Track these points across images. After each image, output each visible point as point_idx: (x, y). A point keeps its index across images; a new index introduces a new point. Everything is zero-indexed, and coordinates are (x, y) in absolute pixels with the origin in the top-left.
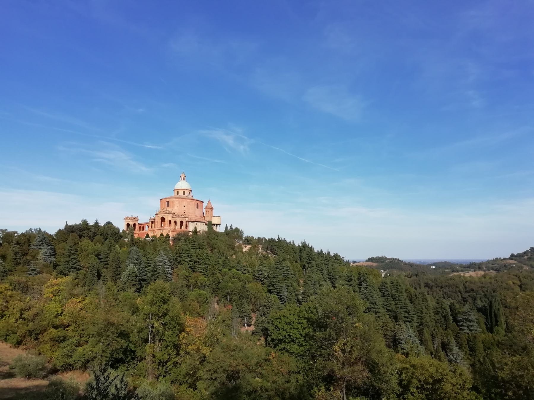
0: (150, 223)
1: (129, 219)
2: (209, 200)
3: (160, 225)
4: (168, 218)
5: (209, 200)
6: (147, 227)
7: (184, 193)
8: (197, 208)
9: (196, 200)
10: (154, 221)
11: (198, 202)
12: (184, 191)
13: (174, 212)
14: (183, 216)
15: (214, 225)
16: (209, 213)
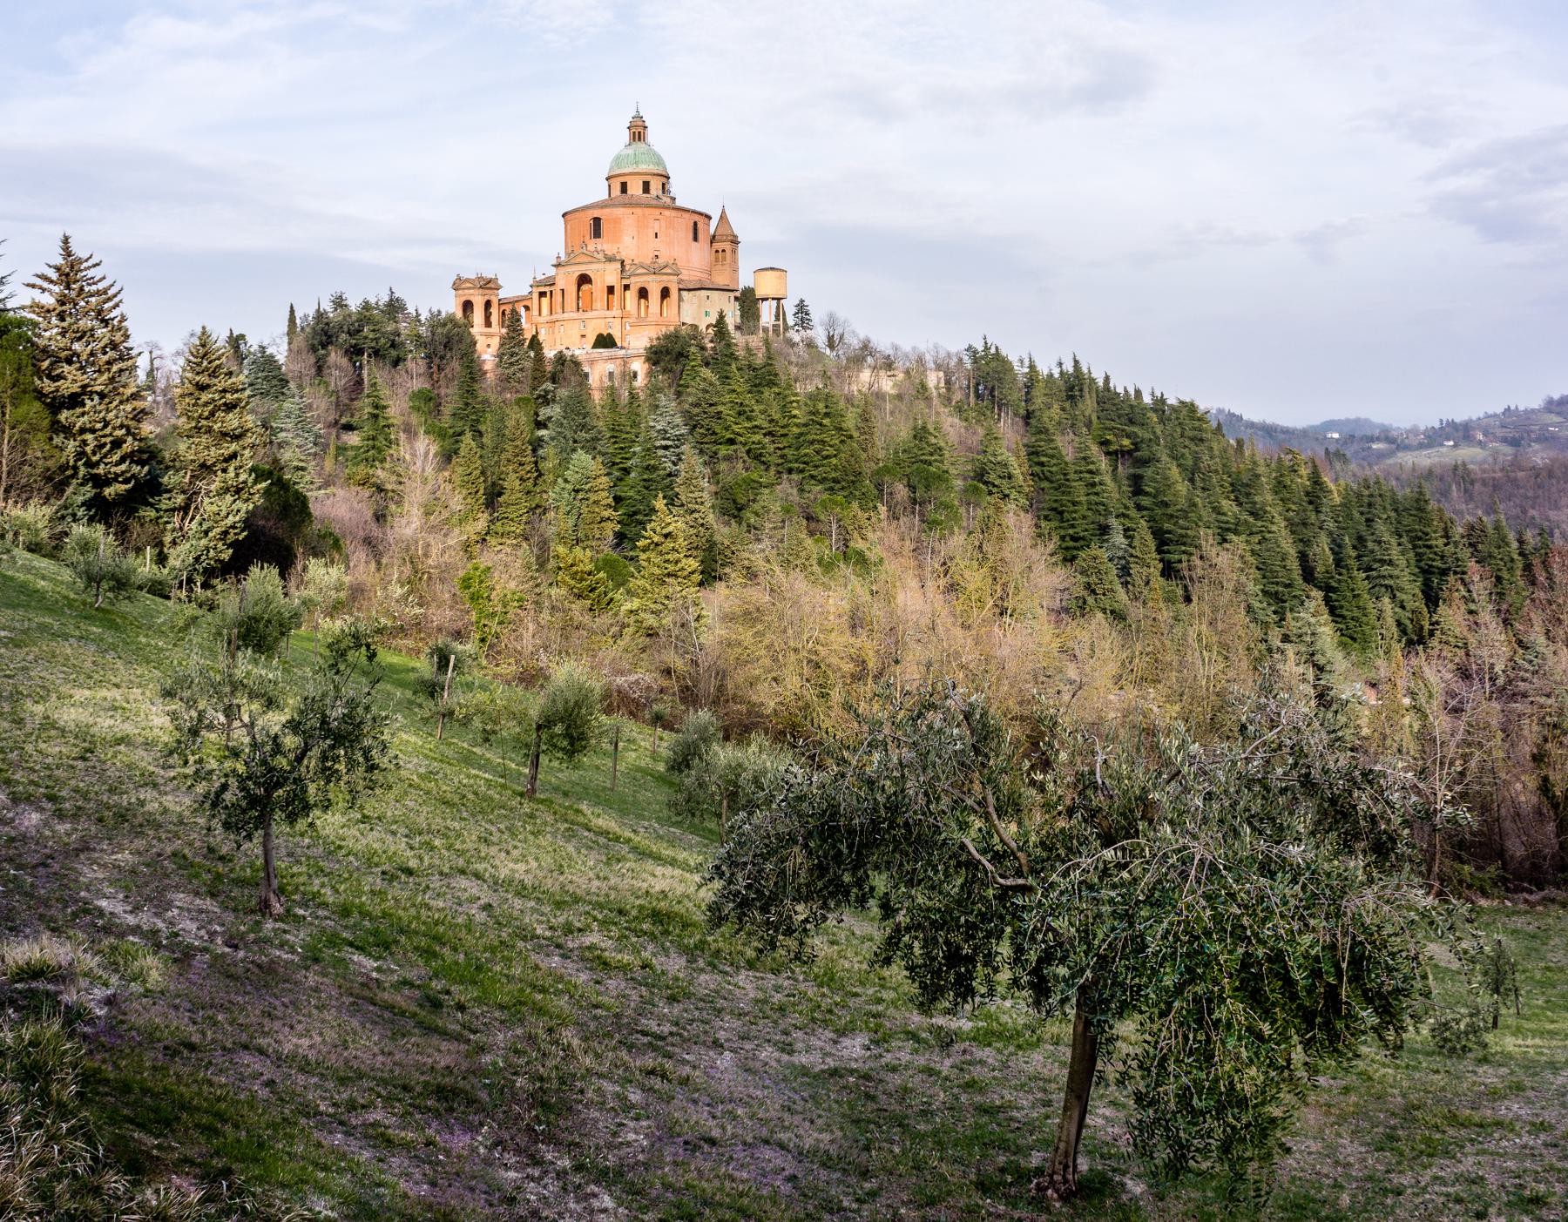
0: (536, 296)
1: (468, 285)
2: (723, 212)
3: (575, 305)
4: (608, 275)
5: (723, 212)
6: (522, 311)
7: (646, 187)
8: (696, 239)
9: (694, 212)
10: (547, 289)
11: (696, 218)
12: (646, 178)
13: (623, 255)
14: (670, 271)
15: (763, 300)
16: (724, 259)
